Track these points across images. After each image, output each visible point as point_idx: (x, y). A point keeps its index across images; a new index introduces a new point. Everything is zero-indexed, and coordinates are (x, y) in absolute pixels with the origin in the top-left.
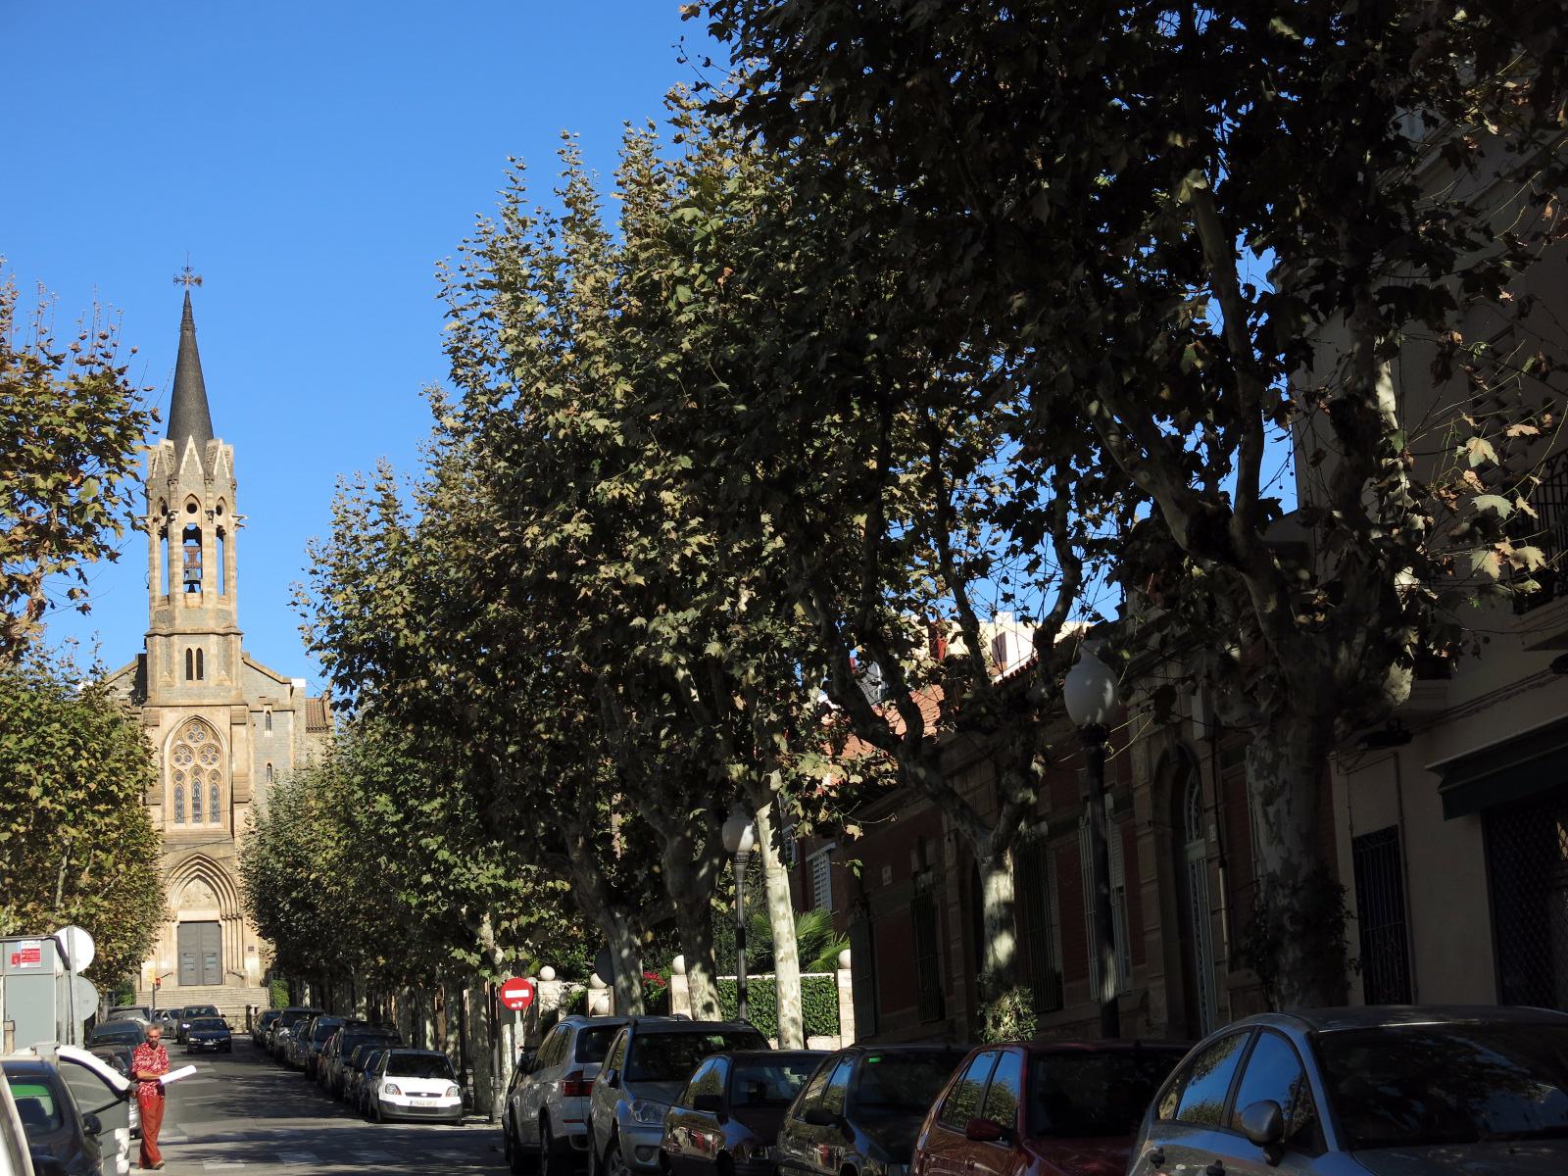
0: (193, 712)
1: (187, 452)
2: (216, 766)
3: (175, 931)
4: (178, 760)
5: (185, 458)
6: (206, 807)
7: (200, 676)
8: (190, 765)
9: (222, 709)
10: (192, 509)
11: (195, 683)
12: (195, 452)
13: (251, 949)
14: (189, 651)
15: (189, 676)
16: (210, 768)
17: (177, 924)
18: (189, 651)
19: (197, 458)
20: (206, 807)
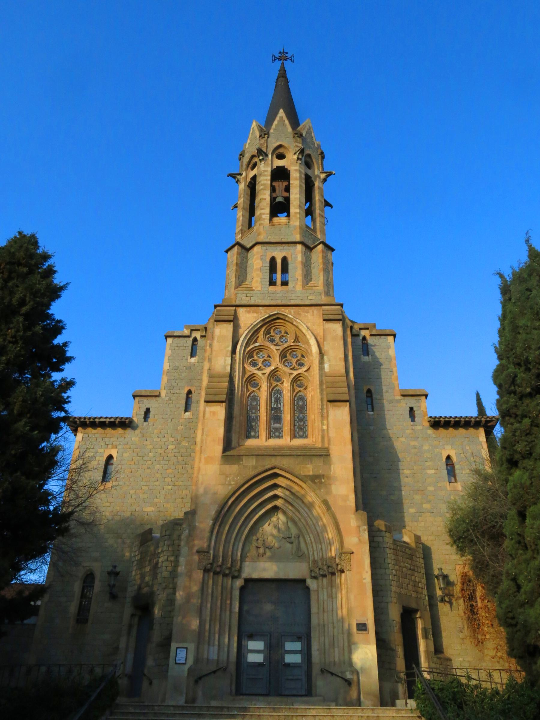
0: (275, 311)
1: (278, 118)
2: (302, 370)
3: (237, 593)
4: (254, 364)
5: (276, 122)
6: (287, 417)
7: (285, 283)
8: (268, 370)
9: (310, 309)
10: (281, 157)
11: (278, 288)
12: (285, 118)
13: (362, 627)
14: (273, 261)
15: (272, 283)
16: (295, 373)
17: (239, 583)
18: (273, 261)
19: (287, 122)
20: (287, 417)
